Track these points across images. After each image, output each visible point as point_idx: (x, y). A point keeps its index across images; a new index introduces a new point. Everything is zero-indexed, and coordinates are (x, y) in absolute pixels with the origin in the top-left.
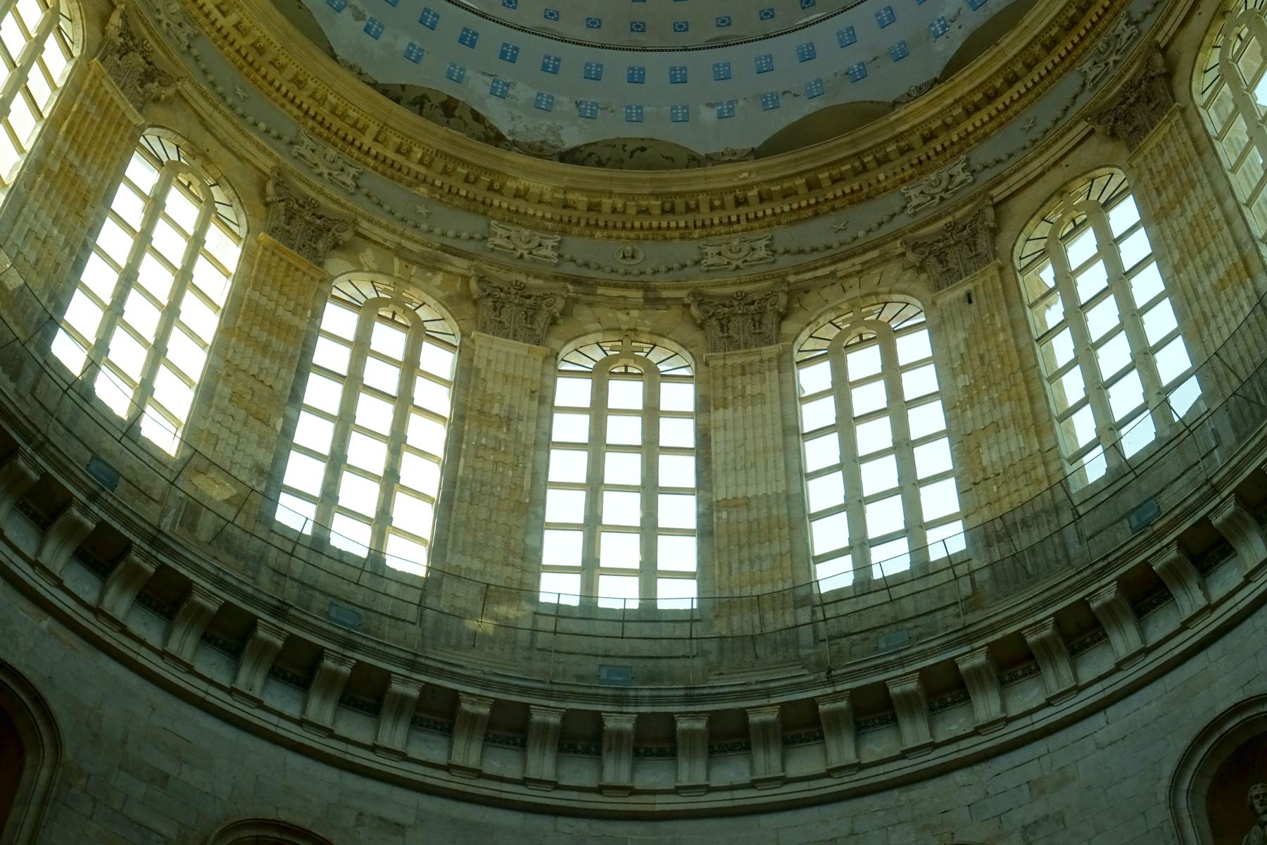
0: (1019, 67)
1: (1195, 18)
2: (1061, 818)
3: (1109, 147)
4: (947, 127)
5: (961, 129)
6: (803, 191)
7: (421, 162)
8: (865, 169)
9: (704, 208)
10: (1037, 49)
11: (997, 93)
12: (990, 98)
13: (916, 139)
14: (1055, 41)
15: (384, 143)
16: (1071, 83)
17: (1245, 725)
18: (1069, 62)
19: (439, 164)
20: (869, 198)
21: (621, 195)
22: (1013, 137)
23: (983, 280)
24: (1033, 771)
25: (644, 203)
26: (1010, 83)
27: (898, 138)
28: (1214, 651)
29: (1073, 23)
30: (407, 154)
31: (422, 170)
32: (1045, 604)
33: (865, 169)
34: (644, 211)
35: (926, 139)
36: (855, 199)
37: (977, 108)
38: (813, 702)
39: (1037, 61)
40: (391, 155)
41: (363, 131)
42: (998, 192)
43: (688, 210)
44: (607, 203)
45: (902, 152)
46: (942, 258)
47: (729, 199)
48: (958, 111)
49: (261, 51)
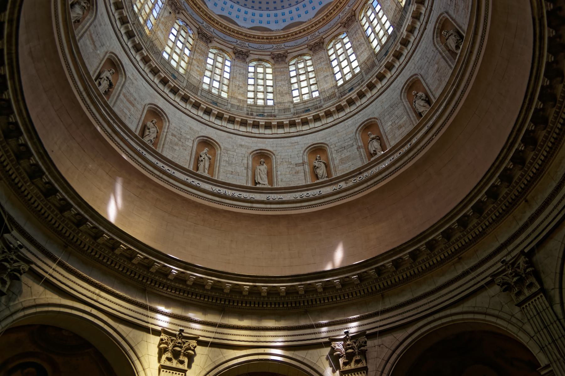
0: (201, 9)
1: (219, 44)
2: (133, 83)
3: (196, 33)
10: (205, 13)
11: (196, 6)
12: (195, 4)
14: (206, 16)
16: (201, 21)
17: (160, 112)
18: (204, 19)
22: (190, 11)
23: (173, 15)
24: (134, 73)
26: (198, 8)
28: (162, 98)
29: (210, 19)
32: (157, 63)
38: (128, 22)
42: (183, 12)
46: (172, 3)
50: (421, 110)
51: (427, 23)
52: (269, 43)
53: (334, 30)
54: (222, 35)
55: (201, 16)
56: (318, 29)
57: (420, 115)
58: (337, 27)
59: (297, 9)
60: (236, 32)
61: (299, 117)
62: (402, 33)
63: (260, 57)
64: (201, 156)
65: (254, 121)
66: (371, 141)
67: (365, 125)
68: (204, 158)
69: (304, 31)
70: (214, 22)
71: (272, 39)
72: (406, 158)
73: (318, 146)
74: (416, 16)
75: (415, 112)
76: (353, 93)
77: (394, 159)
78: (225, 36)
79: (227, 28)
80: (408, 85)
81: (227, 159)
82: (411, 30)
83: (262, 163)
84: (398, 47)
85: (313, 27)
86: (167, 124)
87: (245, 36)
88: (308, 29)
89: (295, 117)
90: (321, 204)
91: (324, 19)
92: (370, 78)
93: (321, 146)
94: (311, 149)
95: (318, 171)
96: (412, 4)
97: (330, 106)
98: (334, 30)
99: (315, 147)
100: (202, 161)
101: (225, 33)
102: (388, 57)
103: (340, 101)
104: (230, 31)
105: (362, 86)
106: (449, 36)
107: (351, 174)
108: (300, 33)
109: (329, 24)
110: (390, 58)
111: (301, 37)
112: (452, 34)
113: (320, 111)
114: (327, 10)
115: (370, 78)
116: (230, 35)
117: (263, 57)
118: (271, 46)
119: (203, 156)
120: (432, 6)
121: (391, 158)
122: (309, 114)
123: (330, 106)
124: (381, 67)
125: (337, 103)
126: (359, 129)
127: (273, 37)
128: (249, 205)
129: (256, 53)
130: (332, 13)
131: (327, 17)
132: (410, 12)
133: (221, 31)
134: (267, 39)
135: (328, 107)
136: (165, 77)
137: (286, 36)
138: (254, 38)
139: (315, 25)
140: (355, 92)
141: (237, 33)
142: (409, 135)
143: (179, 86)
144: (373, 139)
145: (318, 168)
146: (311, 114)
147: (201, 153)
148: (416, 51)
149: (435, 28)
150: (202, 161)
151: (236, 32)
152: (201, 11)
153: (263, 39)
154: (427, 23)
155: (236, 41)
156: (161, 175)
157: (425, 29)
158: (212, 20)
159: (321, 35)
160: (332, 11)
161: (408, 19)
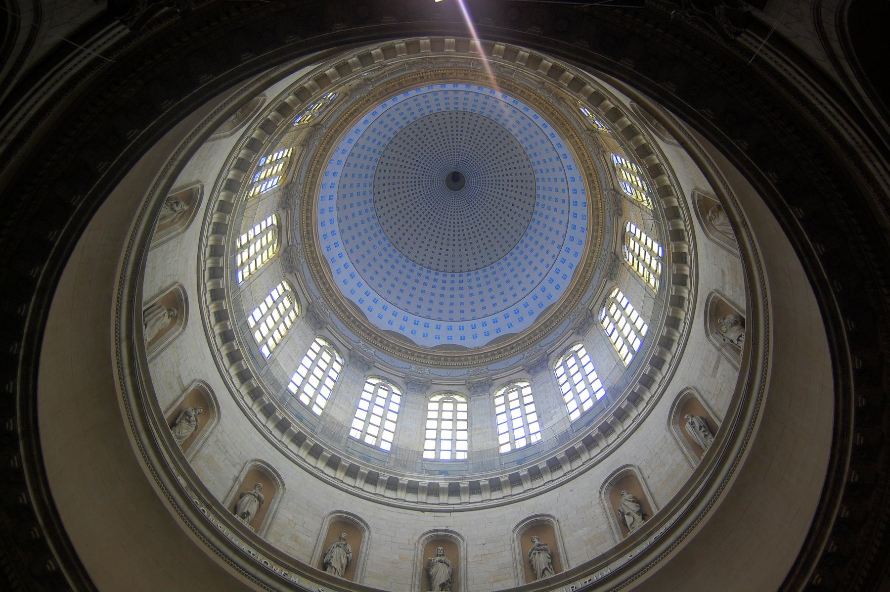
0: (344, 124)
4: (363, 104)
5: (359, 104)
6: (404, 82)
7: (518, 89)
8: (386, 90)
9: (433, 76)
10: (340, 130)
13: (371, 100)
15: (528, 95)
18: (331, 128)
19: (512, 88)
20: (384, 83)
21: (458, 79)
25: (451, 76)
27: (377, 100)
30: (522, 91)
31: (517, 86)
33: (386, 90)
34: (451, 73)
35: (369, 100)
36: (389, 82)
37: (355, 110)
38: (386, 59)
39: (339, 126)
40: (527, 91)
41: (535, 99)
43: (438, 74)
44: (462, 76)
45: (375, 96)
47: (426, 77)
48: (361, 109)
49: (562, 124)
50: (335, 563)
51: (431, 511)
52: (302, 237)
53: (341, 339)
54: (308, 159)
55: (335, 123)
56: (334, 311)
57: (325, 565)
58: (346, 344)
59: (346, 266)
60: (314, 180)
61: (240, 343)
62: (404, 476)
63: (284, 229)
64: (177, 203)
65: (222, 268)
66: (254, 495)
67: (266, 470)
68: (176, 211)
69: (327, 290)
70: (327, 144)
71: (309, 239)
72: (242, 562)
73: (211, 400)
74: (433, 490)
75: (324, 555)
76: (298, 425)
77: (254, 557)
78: (307, 165)
79: (318, 167)
80: (347, 518)
81: (170, 250)
82: (413, 488)
83: (172, 313)
84: (384, 476)
85: (335, 302)
86: (228, 133)
87: (309, 196)
88: (330, 295)
89: (238, 338)
90: (153, 469)
91: (349, 318)
92: (327, 446)
93: (213, 406)
94: (204, 390)
95: (185, 424)
96: (445, 479)
97: (268, 393)
98: (341, 339)
99: (208, 394)
100: (172, 209)
101: (311, 164)
102: (365, 465)
103: (279, 406)
104: (315, 170)
105: (313, 436)
106: (445, 563)
107: (201, 490)
108: (324, 284)
109: (345, 328)
110: (364, 469)
111: (318, 287)
112: (448, 566)
113: (258, 378)
114: (362, 320)
115: (327, 446)
116: (309, 171)
117: (284, 233)
118: (299, 241)
119: (178, 209)
120: (454, 511)
121: (253, 551)
122: (248, 361)
123: (268, 393)
124: (348, 458)
125: (276, 403)
126: (257, 463)
127: (311, 242)
128: (123, 334)
129: (289, 219)
130: (360, 328)
131: (352, 321)
132: (434, 479)
133: (314, 158)
134: (308, 231)
135: (266, 390)
136: (293, 110)
137: (316, 261)
138: (307, 210)
139: (338, 306)
140: (300, 427)
141: (312, 182)
142: (298, 564)
143: (275, 134)
144: (259, 498)
145: (189, 422)
146: (250, 364)
147: (182, 203)
148: (391, 508)
149: (437, 530)
150: (172, 209)
151: (314, 180)
152: (341, 124)
153: (307, 225)
154: (431, 511)
155: (301, 182)
156: (176, 163)
157: (423, 511)
158: (328, 142)
159: (329, 320)
160: (363, 327)
161: (424, 478)
